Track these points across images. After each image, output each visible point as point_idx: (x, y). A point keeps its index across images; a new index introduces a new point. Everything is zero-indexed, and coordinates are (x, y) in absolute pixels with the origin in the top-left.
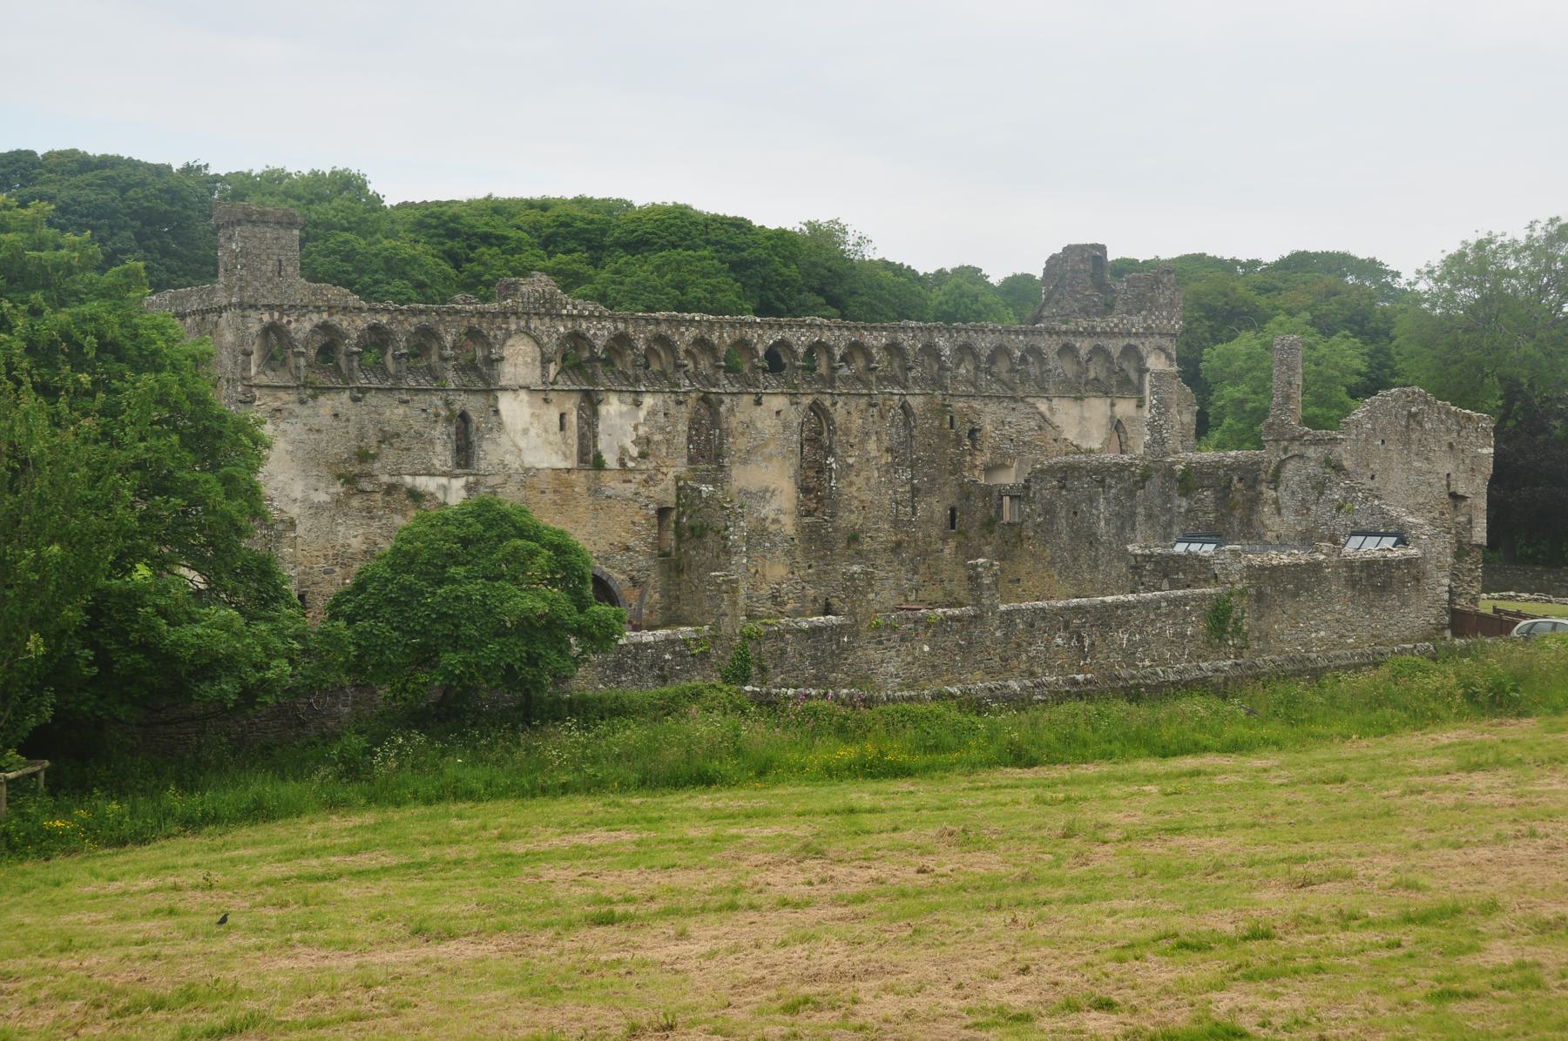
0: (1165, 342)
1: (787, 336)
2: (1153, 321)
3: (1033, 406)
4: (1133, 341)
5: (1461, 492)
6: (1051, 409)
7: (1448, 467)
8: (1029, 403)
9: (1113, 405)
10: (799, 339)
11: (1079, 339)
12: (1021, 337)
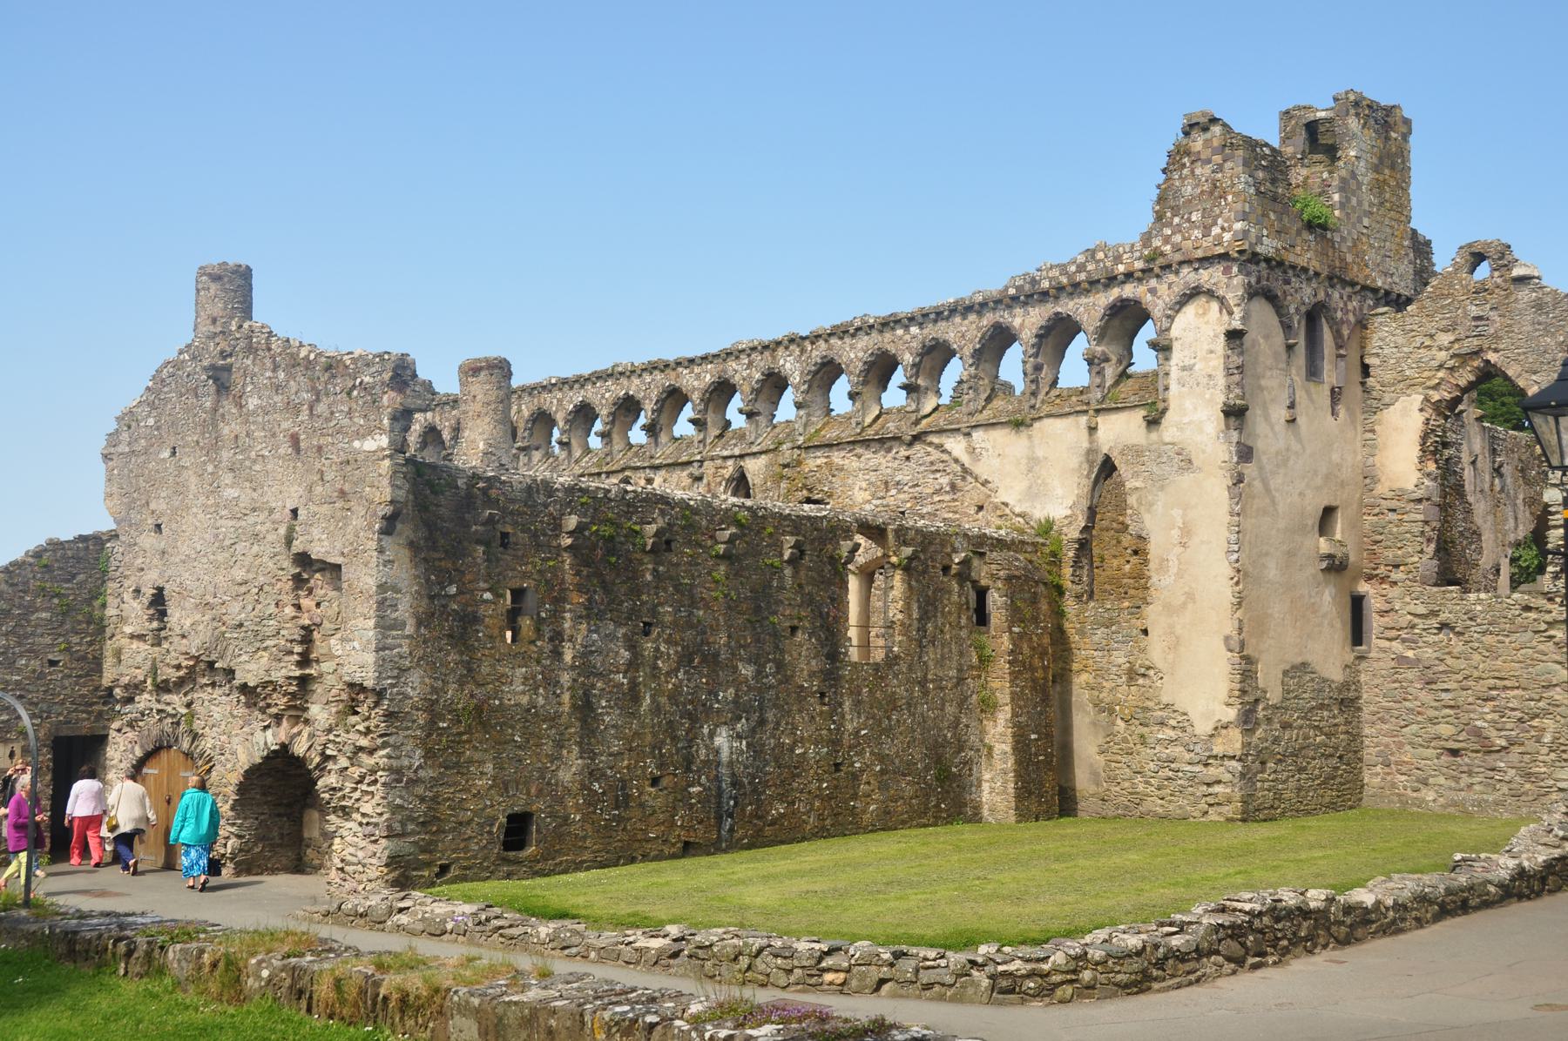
0: (1210, 276)
1: (589, 395)
2: (1167, 240)
3: (940, 447)
4: (1129, 291)
5: (317, 552)
6: (972, 451)
7: (293, 495)
8: (931, 444)
9: (1092, 429)
10: (603, 397)
11: (1018, 311)
12: (914, 330)
